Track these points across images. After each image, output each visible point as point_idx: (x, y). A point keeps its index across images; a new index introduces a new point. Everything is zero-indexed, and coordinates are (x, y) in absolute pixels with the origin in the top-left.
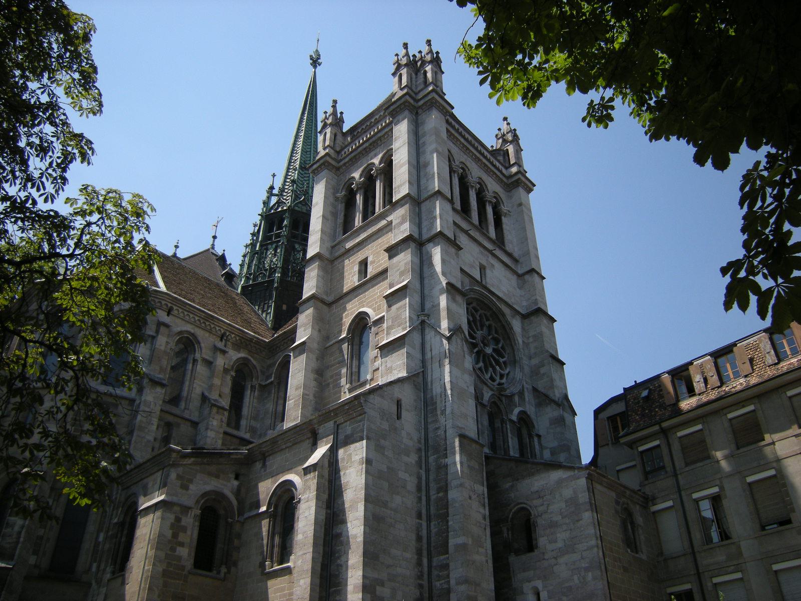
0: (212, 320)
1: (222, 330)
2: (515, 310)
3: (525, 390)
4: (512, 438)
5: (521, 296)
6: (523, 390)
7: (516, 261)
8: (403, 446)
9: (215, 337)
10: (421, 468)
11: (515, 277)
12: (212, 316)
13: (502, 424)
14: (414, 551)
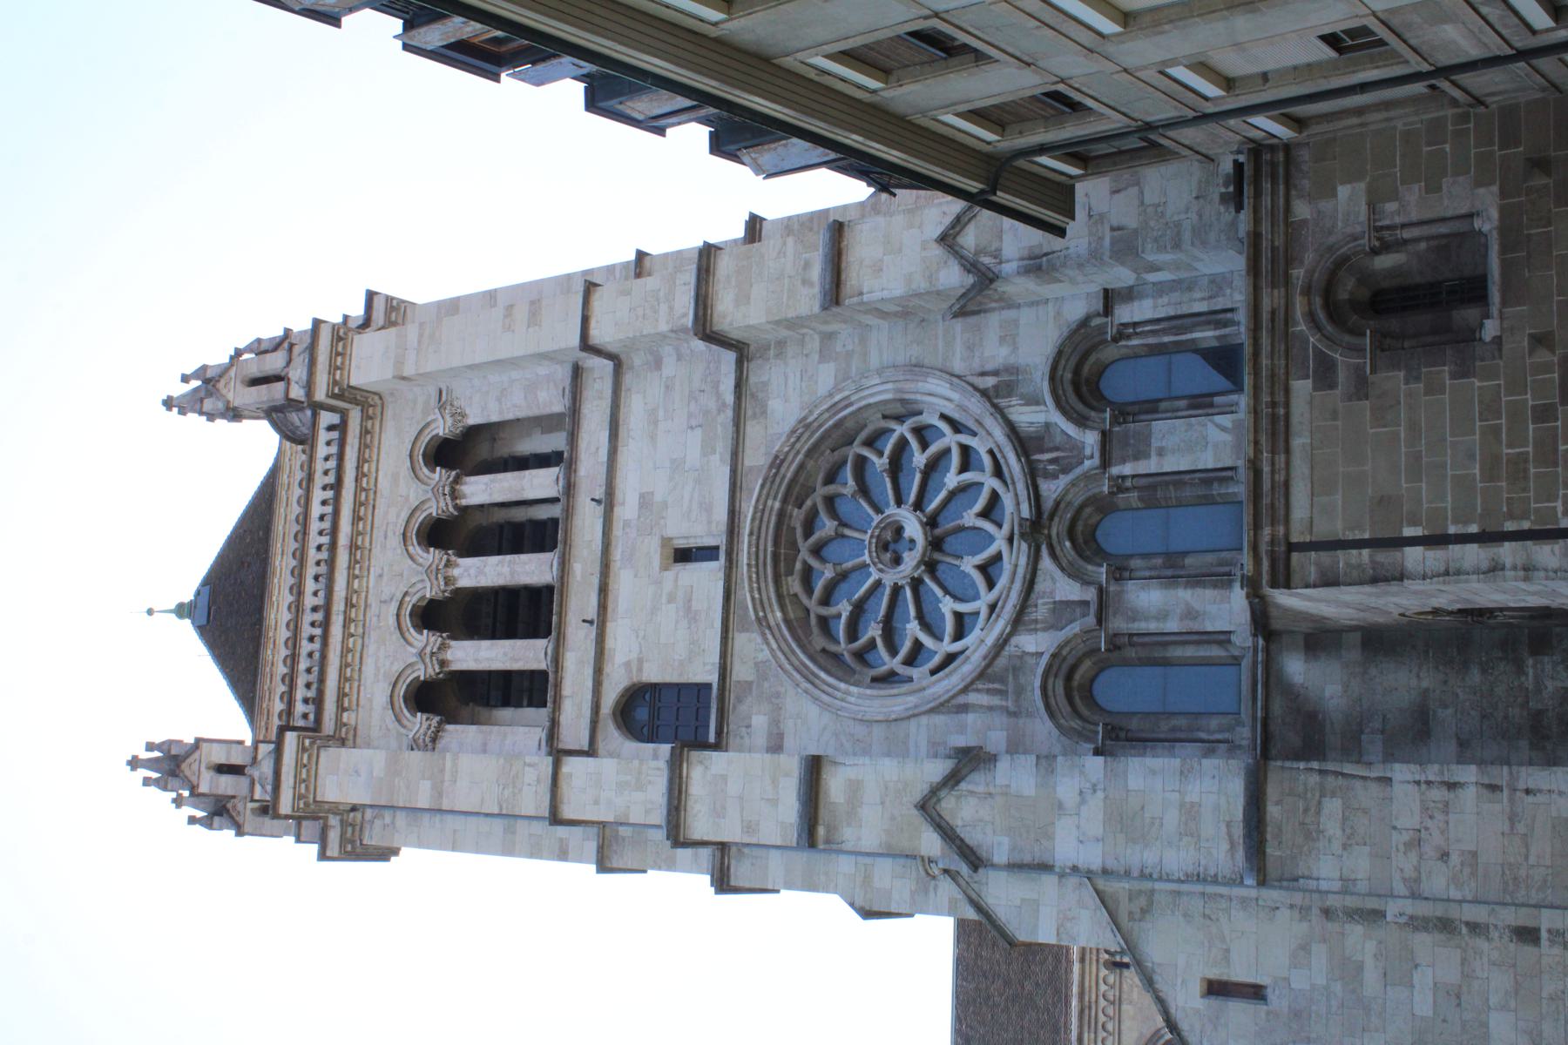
0: (1090, 1008)
1: (1101, 975)
7: (577, 372)
8: (1338, 987)
9: (1125, 987)
10: (1382, 914)
11: (628, 379)
12: (1081, 1012)
13: (1127, 490)
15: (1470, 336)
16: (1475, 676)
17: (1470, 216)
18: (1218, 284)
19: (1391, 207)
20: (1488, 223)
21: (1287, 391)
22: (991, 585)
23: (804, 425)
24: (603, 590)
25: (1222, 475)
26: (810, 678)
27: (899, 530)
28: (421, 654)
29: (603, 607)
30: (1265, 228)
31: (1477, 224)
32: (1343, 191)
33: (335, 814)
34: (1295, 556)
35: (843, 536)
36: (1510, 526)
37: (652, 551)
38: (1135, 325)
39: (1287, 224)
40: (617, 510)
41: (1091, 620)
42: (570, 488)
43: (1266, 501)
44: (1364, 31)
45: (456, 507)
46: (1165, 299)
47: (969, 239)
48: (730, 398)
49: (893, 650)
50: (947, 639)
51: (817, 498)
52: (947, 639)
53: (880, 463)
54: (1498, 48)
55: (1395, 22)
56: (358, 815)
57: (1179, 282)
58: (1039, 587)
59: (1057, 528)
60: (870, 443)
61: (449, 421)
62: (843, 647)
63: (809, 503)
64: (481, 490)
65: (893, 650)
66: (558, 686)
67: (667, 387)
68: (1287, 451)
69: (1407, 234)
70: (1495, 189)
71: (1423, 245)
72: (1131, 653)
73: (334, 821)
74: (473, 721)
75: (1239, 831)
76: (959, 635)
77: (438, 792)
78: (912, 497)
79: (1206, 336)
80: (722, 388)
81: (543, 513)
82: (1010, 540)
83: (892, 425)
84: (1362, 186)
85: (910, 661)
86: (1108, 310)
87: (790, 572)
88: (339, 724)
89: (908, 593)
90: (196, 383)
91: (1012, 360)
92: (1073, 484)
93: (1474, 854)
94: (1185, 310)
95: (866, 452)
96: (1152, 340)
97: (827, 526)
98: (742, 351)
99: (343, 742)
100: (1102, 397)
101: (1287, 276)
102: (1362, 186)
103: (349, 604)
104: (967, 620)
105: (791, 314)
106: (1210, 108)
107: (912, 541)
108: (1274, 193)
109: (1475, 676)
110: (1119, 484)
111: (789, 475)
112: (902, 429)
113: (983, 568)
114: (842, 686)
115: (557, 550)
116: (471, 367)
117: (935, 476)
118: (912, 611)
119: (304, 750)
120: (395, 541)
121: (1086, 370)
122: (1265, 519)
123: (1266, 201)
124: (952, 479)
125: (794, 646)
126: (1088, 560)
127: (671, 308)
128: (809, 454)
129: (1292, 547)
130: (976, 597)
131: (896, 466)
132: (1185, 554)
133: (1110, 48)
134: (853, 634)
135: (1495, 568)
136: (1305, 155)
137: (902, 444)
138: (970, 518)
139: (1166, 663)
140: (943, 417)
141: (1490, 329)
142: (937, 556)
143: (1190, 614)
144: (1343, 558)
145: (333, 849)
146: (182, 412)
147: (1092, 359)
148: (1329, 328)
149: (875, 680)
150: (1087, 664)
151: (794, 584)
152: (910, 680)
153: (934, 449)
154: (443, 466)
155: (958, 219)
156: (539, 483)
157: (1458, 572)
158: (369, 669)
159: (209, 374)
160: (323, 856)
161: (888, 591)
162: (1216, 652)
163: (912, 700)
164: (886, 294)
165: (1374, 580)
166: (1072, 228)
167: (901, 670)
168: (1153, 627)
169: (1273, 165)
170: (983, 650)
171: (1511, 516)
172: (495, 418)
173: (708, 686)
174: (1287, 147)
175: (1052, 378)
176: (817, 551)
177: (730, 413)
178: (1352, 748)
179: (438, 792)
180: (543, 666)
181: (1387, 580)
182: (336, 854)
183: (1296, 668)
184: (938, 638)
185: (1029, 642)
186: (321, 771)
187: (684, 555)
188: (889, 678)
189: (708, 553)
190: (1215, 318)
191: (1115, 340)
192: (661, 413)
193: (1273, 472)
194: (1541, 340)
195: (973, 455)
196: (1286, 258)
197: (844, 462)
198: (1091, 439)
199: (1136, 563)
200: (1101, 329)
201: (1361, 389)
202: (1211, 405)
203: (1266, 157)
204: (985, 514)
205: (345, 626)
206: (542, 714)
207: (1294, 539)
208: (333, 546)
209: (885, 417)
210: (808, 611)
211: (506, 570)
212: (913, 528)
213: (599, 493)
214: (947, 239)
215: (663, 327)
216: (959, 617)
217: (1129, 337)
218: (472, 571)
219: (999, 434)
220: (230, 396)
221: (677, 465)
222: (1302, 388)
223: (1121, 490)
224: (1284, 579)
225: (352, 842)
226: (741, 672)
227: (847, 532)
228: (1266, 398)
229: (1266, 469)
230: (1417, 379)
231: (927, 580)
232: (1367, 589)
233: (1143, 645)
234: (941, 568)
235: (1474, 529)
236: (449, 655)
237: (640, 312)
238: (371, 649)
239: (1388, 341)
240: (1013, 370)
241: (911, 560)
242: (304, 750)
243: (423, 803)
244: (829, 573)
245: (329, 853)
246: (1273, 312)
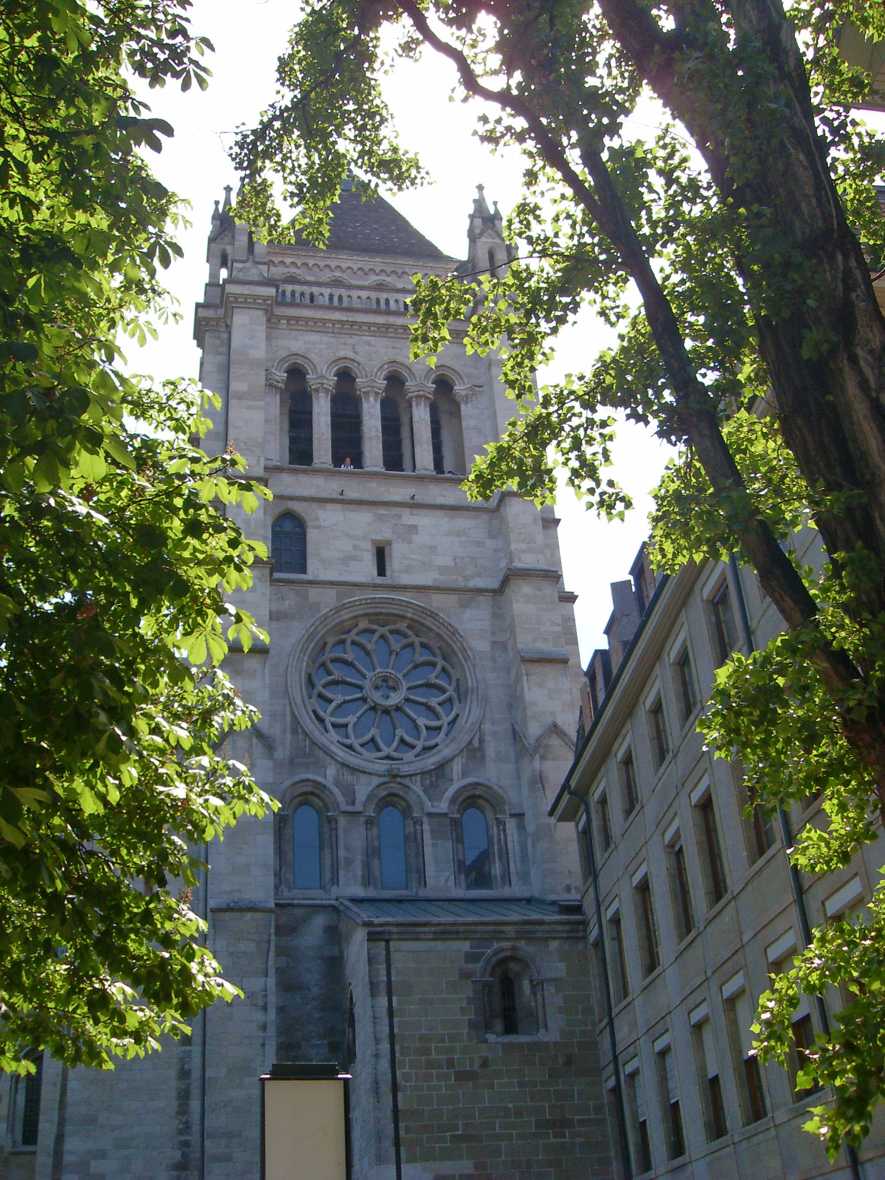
2: (471, 590)
3: (487, 738)
4: (434, 845)
5: (496, 551)
6: (481, 741)
11: (485, 517)
14: (174, 1094)
15: (488, 1027)
16: (317, 1015)
17: (546, 1027)
18: (525, 877)
19: (553, 990)
20: (542, 1036)
21: (465, 939)
22: (362, 745)
23: (455, 632)
24: (360, 503)
25: (422, 881)
26: (310, 638)
27: (394, 689)
28: (322, 377)
29: (351, 502)
30: (547, 927)
31: (542, 1031)
32: (562, 966)
33: (225, 314)
34: (383, 943)
35: (391, 654)
36: (397, 1048)
37: (384, 533)
38: (505, 830)
39: (547, 939)
40: (407, 511)
41: (344, 807)
42: (421, 478)
43: (411, 929)
44: (626, 995)
45: (411, 398)
46: (517, 847)
47: (555, 741)
48: (471, 584)
49: (325, 686)
50: (333, 719)
51: (413, 638)
52: (333, 719)
53: (432, 677)
54: (620, 1047)
55: (630, 1007)
56: (223, 329)
57: (527, 855)
58: (362, 776)
59: (395, 788)
60: (444, 669)
61: (463, 393)
62: (328, 655)
63: (410, 633)
64: (421, 415)
65: (325, 686)
66: (304, 472)
67: (479, 542)
68: (435, 939)
69: (539, 997)
70: (559, 1039)
71: (533, 1004)
72: (326, 829)
73: (221, 312)
74: (281, 413)
75: (236, 896)
76: (334, 725)
77: (241, 396)
78: (412, 697)
79: (497, 869)
80: (478, 579)
81: (407, 462)
82: (388, 757)
83: (454, 683)
84: (564, 975)
85: (320, 696)
86: (512, 815)
87: (371, 622)
88: (279, 318)
89: (359, 695)
90: (492, 212)
91: (488, 759)
92: (418, 796)
93: (231, 1019)
94: (511, 860)
95: (439, 668)
96: (495, 839)
97: (396, 644)
98: (499, 592)
99: (269, 320)
100: (465, 810)
101: (521, 939)
102: (564, 975)
103: (354, 323)
104: (343, 730)
105: (518, 630)
106: (602, 910)
107: (388, 697)
108: (563, 931)
109: (317, 1015)
110: (418, 822)
111: (426, 622)
112: (451, 691)
113: (373, 740)
114: (306, 658)
115: (383, 470)
116: (495, 413)
117: (423, 708)
118: (347, 698)
119: (265, 300)
120: (391, 355)
121: (481, 801)
122: (401, 929)
123: (559, 928)
124: (422, 722)
125: (329, 627)
126: (377, 804)
127: (524, 551)
128: (438, 635)
129: (387, 941)
130: (356, 737)
131: (429, 686)
132: (380, 858)
133: (627, 877)
134: (334, 660)
135: (377, 1041)
136: (580, 946)
137: (443, 691)
138: (400, 732)
139: (321, 848)
140: (457, 716)
141: (491, 1037)
142: (379, 712)
143: (349, 862)
144: (382, 968)
145: (203, 313)
146: (475, 201)
147: (486, 804)
148: (494, 960)
149: (309, 675)
150: (320, 804)
151: (363, 624)
152: (310, 698)
153: (439, 709)
154: (436, 389)
155: (565, 734)
156: (424, 457)
157: (375, 1023)
158: (314, 337)
159: (497, 222)
160: (198, 306)
161: (359, 683)
162: (328, 875)
163: (299, 700)
164: (526, 690)
165: (371, 983)
166: (553, 820)
167: (315, 693)
168: (341, 842)
169: (577, 931)
170: (327, 743)
171: (402, 1048)
172: (464, 424)
173: (304, 571)
174: (585, 938)
175: (477, 784)
176: (382, 637)
177: (462, 584)
178: (280, 952)
179: (241, 396)
180: (315, 461)
181: (371, 989)
182: (200, 315)
183: (319, 921)
184: (332, 714)
185: (332, 771)
186: (252, 312)
187: (381, 555)
188: (310, 683)
189: (381, 571)
190: (506, 877)
191: (497, 819)
192: (463, 539)
193: (424, 933)
194: (485, 1063)
195: (434, 733)
196: (530, 938)
197: (434, 656)
198: (443, 806)
199: (375, 831)
200: (503, 811)
201: (465, 975)
202: (459, 873)
203: (581, 927)
204: (402, 741)
205: (339, 322)
206: (286, 465)
207: (391, 943)
208: (388, 312)
209: (458, 680)
210: (348, 632)
211: (373, 434)
212: (395, 699)
213: (419, 499)
214: (555, 729)
215: (514, 546)
216: (346, 726)
217: (498, 827)
218: (372, 410)
219: (446, 752)
220: (484, 239)
221: (433, 549)
222: (466, 946)
223: (415, 823)
224: (373, 937)
225: (207, 325)
226: (314, 594)
227: (393, 657)
228: (461, 929)
229: (426, 929)
230: (468, 1003)
231: (366, 707)
232: (367, 979)
233: (331, 836)
234: (372, 713)
235: (396, 1031)
236: (321, 395)
237: (523, 531)
238: (326, 339)
239: (487, 988)
240: (483, 758)
241: (377, 697)
242: (265, 300)
243: (235, 386)
244: (370, 646)
245: (200, 309)
246: (503, 932)
